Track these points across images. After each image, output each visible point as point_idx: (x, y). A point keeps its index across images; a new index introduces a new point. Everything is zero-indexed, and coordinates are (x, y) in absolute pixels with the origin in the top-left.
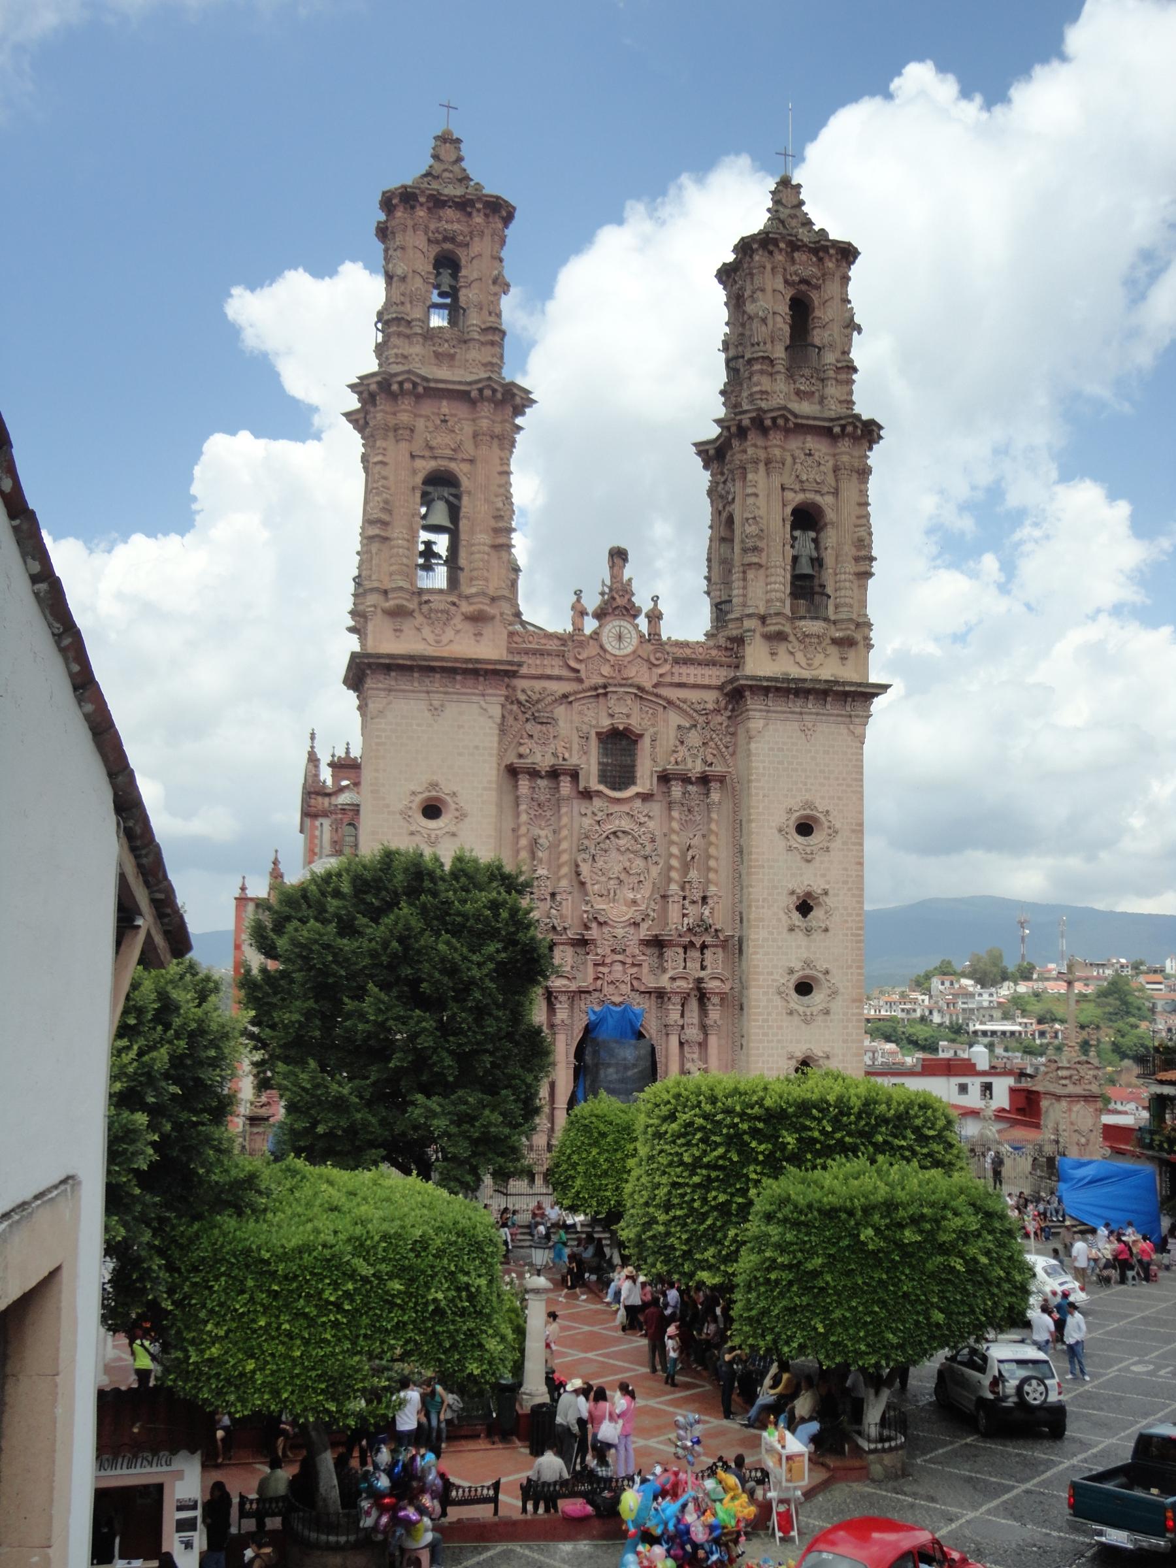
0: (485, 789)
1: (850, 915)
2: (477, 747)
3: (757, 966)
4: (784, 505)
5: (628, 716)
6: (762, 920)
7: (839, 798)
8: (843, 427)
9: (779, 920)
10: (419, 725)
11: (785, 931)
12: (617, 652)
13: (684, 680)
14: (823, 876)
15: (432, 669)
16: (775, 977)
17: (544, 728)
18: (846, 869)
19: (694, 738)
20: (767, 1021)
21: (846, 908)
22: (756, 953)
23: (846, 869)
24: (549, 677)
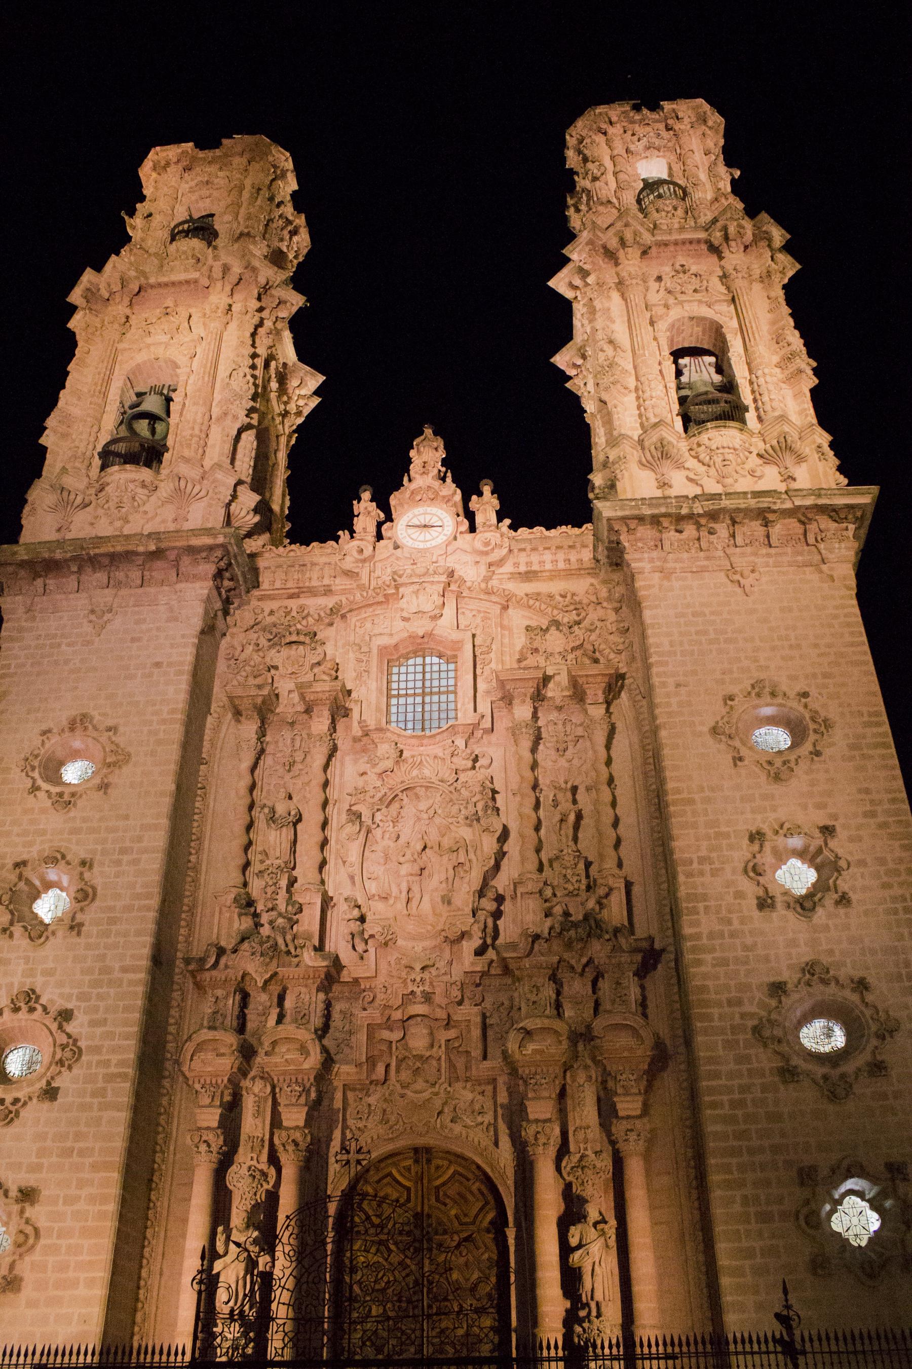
0: (164, 722)
1: (897, 873)
2: (158, 665)
3: (703, 989)
4: (652, 323)
5: (435, 618)
6: (705, 897)
7: (825, 676)
8: (725, 229)
9: (739, 895)
10: (69, 645)
11: (756, 913)
12: (421, 546)
13: (535, 567)
14: (820, 806)
15: (94, 562)
16: (748, 1008)
17: (293, 652)
18: (867, 791)
19: (556, 641)
20: (741, 1104)
21: (882, 861)
22: (699, 962)
23: (867, 791)
24: (312, 592)
